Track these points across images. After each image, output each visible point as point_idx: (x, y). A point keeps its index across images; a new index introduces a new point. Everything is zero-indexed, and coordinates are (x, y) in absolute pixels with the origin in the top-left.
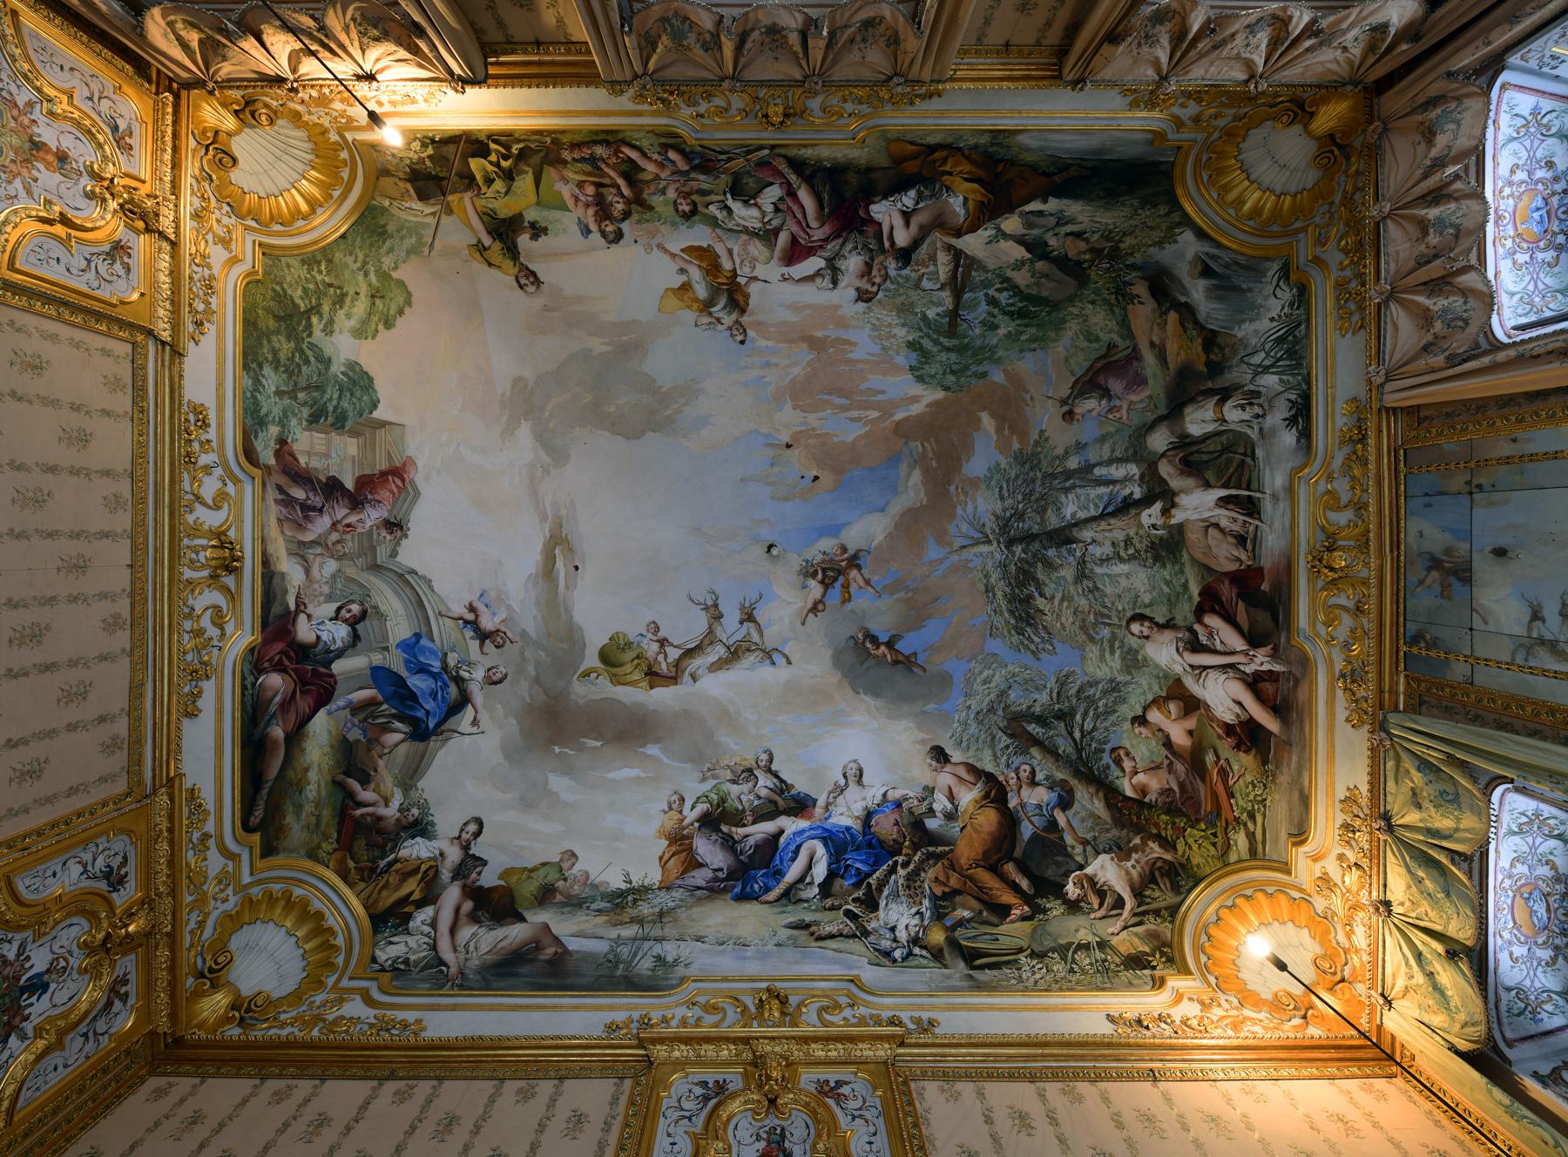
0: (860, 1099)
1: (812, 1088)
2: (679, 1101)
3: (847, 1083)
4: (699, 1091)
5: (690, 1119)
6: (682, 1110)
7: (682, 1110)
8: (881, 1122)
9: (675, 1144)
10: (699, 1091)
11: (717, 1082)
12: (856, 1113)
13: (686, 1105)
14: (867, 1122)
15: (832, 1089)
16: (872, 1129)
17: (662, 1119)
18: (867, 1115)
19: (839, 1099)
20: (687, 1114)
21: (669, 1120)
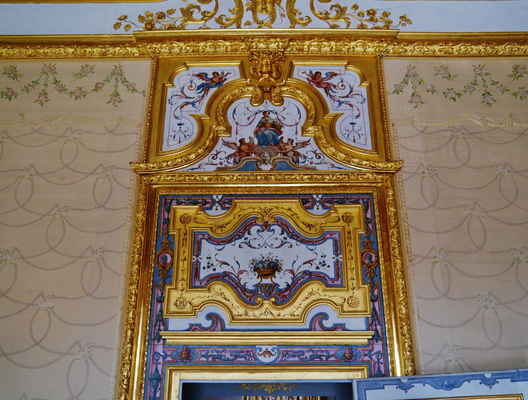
0: (348, 90)
3: (336, 75)
4: (199, 81)
5: (193, 104)
6: (187, 97)
7: (187, 97)
8: (365, 108)
10: (199, 81)
13: (187, 92)
14: (351, 105)
16: (356, 113)
17: (168, 106)
19: (328, 88)
21: (174, 107)
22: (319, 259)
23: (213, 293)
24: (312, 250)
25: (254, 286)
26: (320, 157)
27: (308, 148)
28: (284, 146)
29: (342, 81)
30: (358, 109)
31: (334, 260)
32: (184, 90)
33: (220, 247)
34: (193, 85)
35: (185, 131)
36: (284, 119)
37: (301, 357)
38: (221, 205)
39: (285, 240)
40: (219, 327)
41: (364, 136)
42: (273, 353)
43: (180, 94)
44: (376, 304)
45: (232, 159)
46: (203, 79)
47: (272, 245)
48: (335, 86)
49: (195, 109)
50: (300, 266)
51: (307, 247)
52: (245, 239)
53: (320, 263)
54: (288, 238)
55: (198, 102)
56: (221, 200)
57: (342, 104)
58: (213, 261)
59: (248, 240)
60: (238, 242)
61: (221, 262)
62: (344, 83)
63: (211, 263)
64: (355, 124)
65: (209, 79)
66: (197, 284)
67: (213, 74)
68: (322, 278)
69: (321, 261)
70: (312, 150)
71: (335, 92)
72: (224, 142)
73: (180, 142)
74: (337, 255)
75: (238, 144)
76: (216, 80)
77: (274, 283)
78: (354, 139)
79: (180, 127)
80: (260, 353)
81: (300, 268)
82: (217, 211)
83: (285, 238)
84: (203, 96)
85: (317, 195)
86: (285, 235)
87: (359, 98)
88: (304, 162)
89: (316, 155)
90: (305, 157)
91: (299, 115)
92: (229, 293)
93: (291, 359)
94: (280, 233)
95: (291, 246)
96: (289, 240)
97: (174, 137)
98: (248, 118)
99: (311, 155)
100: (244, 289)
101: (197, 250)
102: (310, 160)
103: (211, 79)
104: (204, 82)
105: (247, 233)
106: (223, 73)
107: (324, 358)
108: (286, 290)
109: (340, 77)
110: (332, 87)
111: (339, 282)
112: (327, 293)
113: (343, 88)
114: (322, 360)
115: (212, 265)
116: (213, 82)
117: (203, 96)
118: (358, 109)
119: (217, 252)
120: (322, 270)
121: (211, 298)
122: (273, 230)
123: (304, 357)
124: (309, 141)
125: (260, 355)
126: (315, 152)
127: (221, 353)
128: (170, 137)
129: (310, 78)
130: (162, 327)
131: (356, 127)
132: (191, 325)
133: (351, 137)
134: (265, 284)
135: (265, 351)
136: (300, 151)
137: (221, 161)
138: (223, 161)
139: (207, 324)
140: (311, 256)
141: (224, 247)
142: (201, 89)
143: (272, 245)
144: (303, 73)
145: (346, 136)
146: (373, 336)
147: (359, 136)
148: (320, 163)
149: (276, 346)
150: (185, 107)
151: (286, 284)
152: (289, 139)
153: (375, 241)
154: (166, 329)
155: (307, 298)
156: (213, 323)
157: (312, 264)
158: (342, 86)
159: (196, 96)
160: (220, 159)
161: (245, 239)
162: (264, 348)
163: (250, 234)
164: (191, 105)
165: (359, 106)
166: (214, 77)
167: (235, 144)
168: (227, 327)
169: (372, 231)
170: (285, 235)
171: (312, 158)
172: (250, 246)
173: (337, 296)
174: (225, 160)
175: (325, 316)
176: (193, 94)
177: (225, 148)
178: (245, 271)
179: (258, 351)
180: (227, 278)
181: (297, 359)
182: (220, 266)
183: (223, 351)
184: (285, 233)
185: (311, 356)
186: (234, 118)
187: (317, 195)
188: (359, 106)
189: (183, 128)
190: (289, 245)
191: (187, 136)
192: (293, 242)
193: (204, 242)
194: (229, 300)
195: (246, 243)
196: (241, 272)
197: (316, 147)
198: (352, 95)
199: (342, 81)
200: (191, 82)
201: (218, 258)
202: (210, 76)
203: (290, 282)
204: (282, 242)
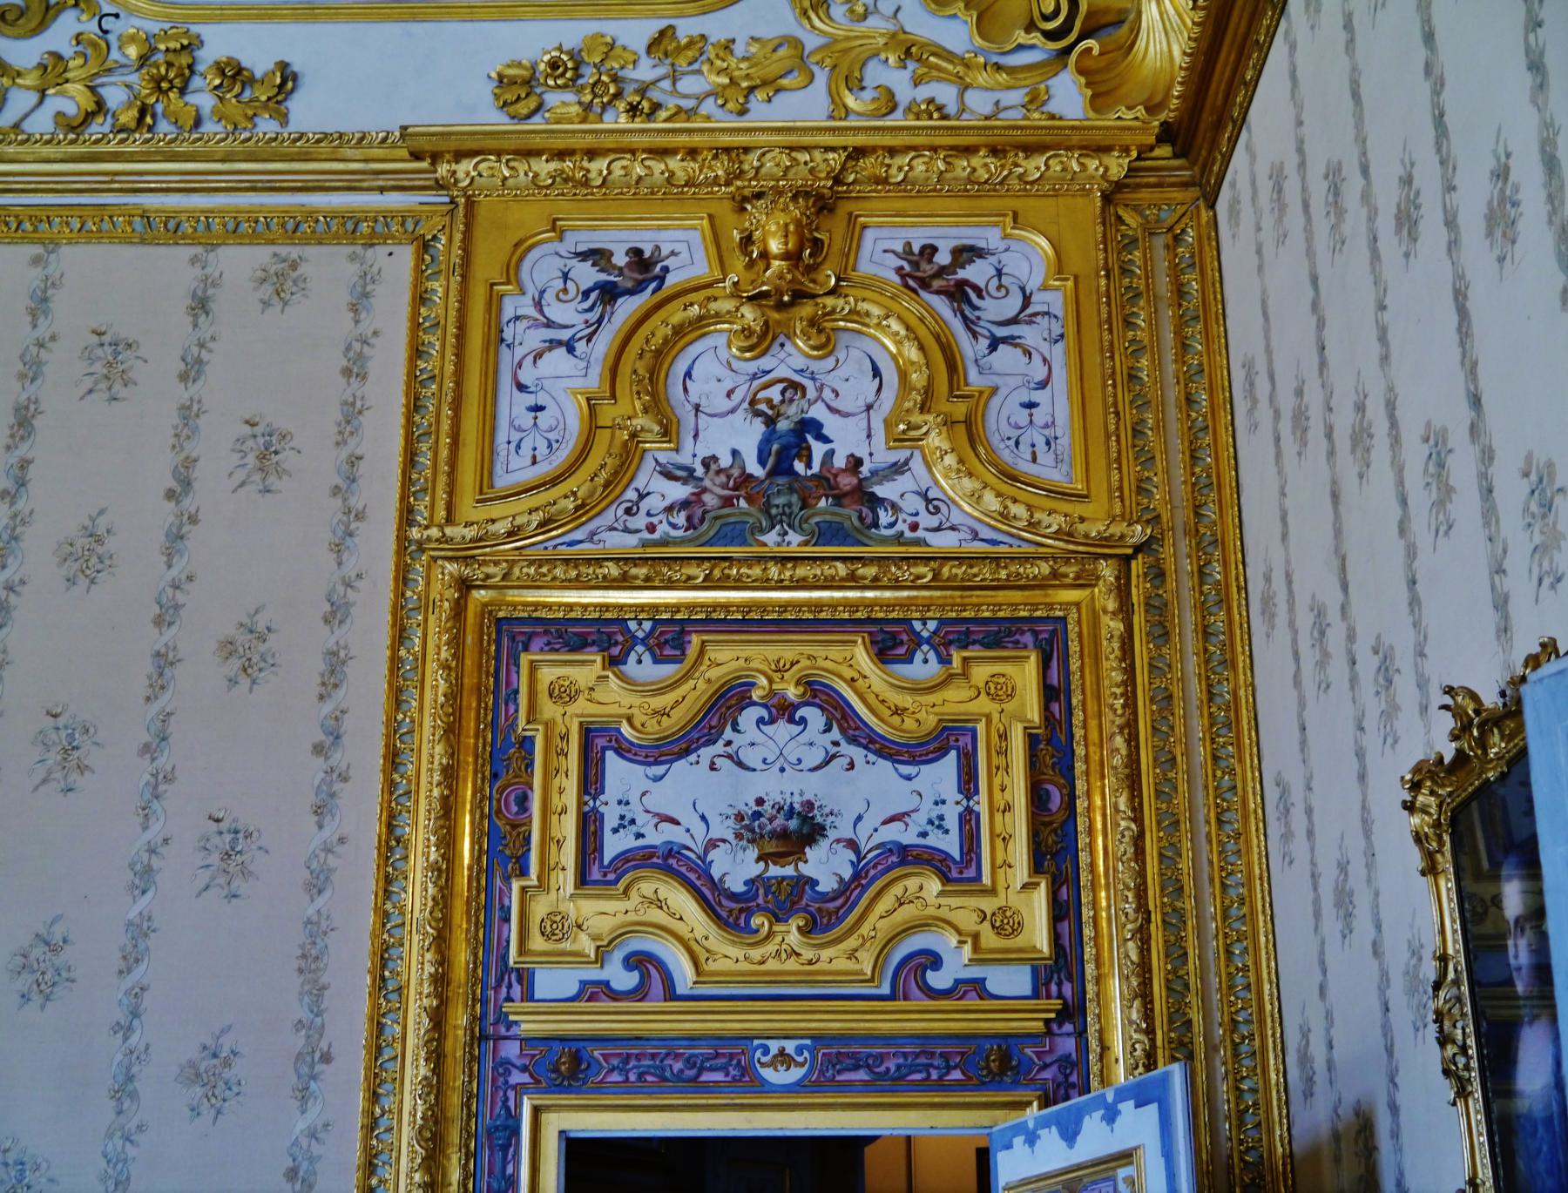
2: (538, 305)
4: (587, 274)
6: (550, 324)
7: (550, 324)
9: (539, 408)
10: (587, 274)
11: (636, 252)
12: (1001, 332)
13: (555, 312)
15: (942, 271)
16: (1040, 372)
20: (565, 335)
22: (927, 810)
24: (909, 778)
25: (746, 883)
29: (999, 273)
33: (659, 770)
37: (877, 1070)
40: (657, 986)
42: (800, 1059)
46: (602, 270)
47: (800, 761)
50: (876, 830)
51: (896, 769)
52: (725, 746)
53: (931, 822)
54: (843, 742)
55: (584, 341)
57: (1001, 347)
58: (635, 810)
59: (734, 746)
60: (706, 753)
62: (1005, 280)
63: (629, 817)
69: (934, 815)
73: (534, 462)
77: (804, 876)
78: (1034, 454)
79: (536, 418)
80: (764, 1059)
81: (874, 835)
83: (836, 744)
84: (600, 321)
85: (924, 621)
86: (835, 734)
91: (877, 380)
92: (681, 900)
94: (822, 728)
95: (852, 766)
101: (591, 781)
104: (603, 277)
105: (728, 728)
109: (992, 259)
110: (973, 296)
113: (1003, 291)
114: (929, 1074)
115: (633, 822)
117: (600, 321)
119: (649, 785)
120: (935, 840)
121: (632, 917)
123: (882, 1069)
125: (763, 1065)
127: (662, 1061)
129: (907, 268)
131: (1040, 415)
132: (584, 984)
134: (776, 878)
139: (626, 980)
141: (667, 771)
142: (593, 296)
143: (800, 761)
145: (1012, 443)
149: (808, 1042)
150: (547, 356)
155: (890, 913)
157: (907, 825)
158: (999, 287)
159: (578, 320)
161: (725, 746)
162: (774, 1050)
163: (739, 731)
164: (563, 350)
172: (740, 764)
175: (935, 961)
176: (568, 313)
178: (724, 841)
179: (758, 1054)
180: (672, 861)
181: (862, 1075)
182: (656, 826)
187: (924, 621)
190: (848, 760)
191: (555, 446)
192: (857, 753)
193: (610, 755)
194: (681, 919)
195: (729, 757)
196: (712, 844)
198: (1031, 315)
199: (999, 273)
202: (620, 259)
203: (847, 873)
204: (827, 752)
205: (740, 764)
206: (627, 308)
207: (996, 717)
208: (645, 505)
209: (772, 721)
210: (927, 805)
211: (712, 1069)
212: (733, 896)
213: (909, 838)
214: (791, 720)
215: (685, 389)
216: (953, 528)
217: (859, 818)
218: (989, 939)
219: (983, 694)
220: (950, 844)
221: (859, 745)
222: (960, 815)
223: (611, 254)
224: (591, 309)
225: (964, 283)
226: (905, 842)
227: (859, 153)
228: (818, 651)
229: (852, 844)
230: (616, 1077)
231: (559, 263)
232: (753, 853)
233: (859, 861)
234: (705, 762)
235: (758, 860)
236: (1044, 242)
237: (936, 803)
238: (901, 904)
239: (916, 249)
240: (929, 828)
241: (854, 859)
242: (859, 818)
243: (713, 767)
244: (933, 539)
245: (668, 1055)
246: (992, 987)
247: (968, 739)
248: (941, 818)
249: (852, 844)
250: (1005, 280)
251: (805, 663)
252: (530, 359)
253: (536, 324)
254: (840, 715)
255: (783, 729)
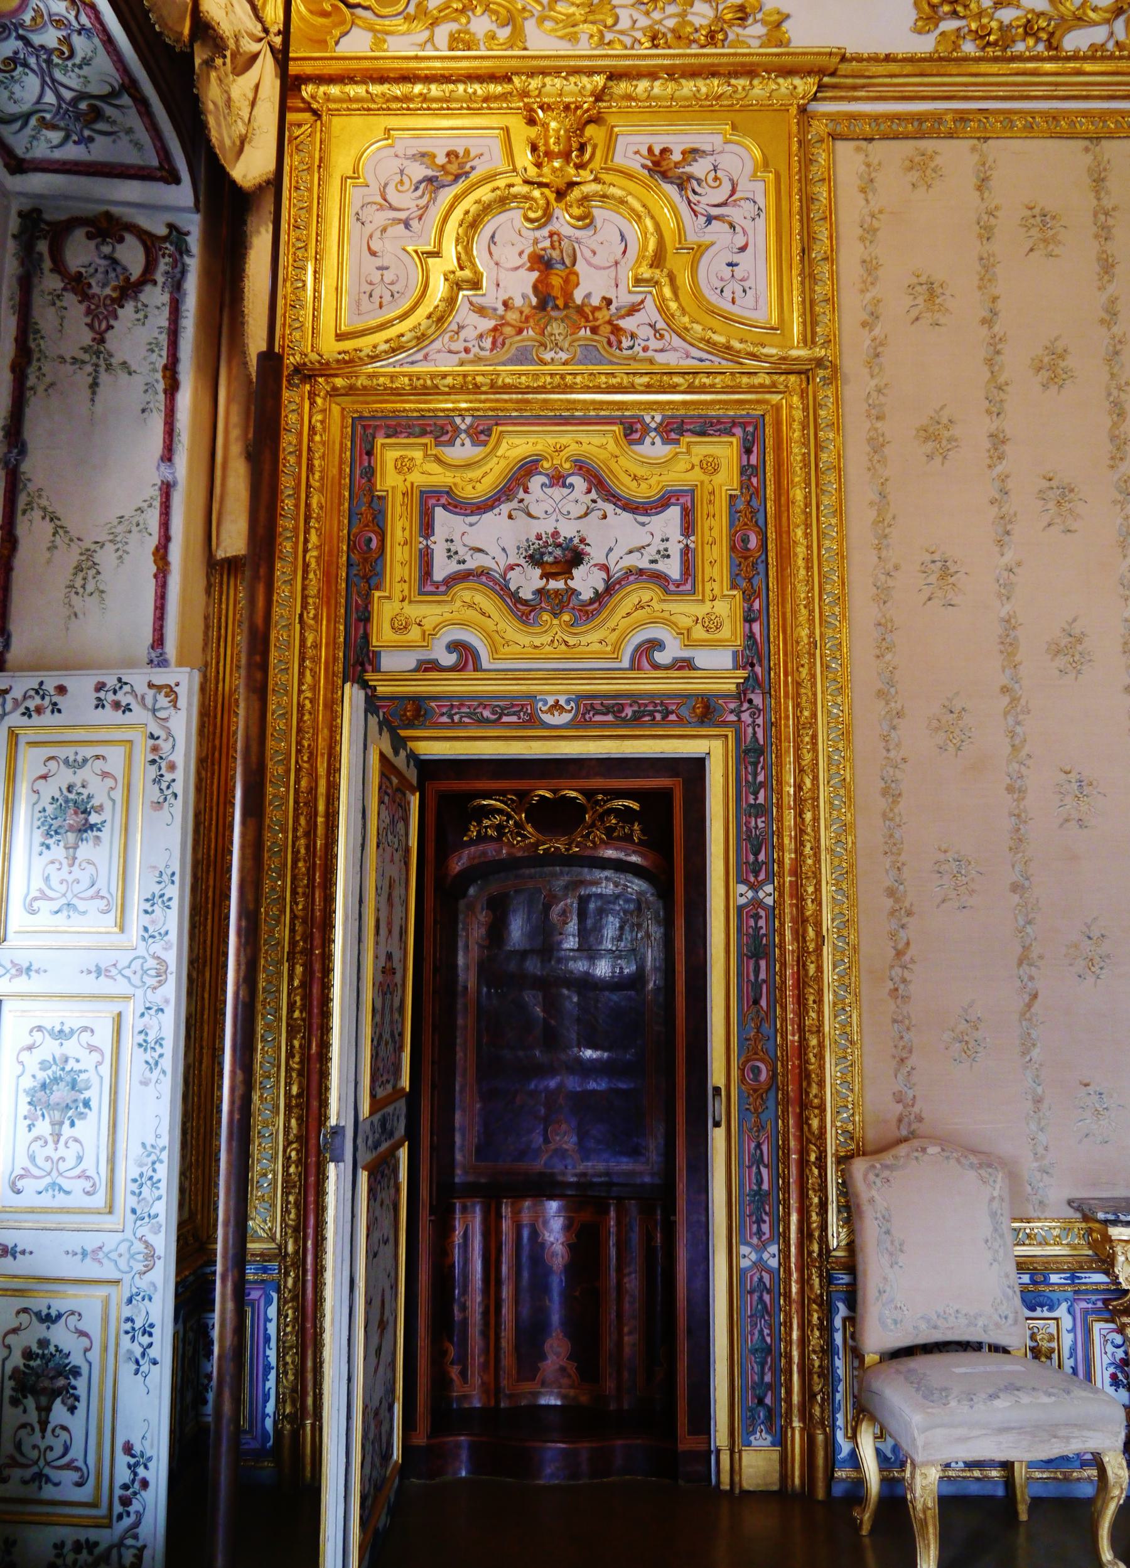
0: (727, 188)
1: (635, 164)
4: (419, 171)
5: (407, 225)
6: (392, 208)
7: (392, 208)
14: (732, 226)
16: (740, 241)
18: (733, 213)
20: (403, 215)
23: (458, 603)
24: (643, 524)
25: (534, 593)
26: (662, 336)
27: (639, 317)
28: (593, 313)
30: (745, 233)
31: (682, 546)
32: (387, 190)
34: (405, 179)
35: (392, 283)
36: (594, 253)
38: (470, 436)
39: (594, 505)
41: (753, 291)
42: (568, 708)
43: (379, 200)
44: (756, 627)
45: (490, 340)
46: (427, 168)
48: (699, 181)
49: (409, 234)
56: (470, 427)
57: (714, 222)
58: (457, 546)
59: (525, 503)
60: (505, 508)
61: (471, 549)
62: (719, 174)
63: (453, 549)
64: (737, 265)
65: (438, 166)
66: (429, 588)
67: (448, 155)
68: (659, 578)
70: (648, 321)
71: (700, 195)
72: (471, 303)
73: (381, 307)
74: (687, 536)
75: (501, 310)
76: (453, 168)
82: (462, 450)
83: (594, 501)
86: (593, 495)
87: (748, 205)
88: (631, 348)
89: (656, 331)
90: (633, 336)
93: (598, 718)
94: (585, 490)
95: (605, 517)
96: (601, 504)
97: (371, 296)
98: (521, 254)
99: (645, 332)
100: (515, 597)
101: (427, 527)
102: (643, 344)
103: (443, 167)
106: (467, 152)
107: (658, 716)
108: (592, 601)
109: (710, 159)
110: (694, 183)
111: (688, 587)
112: (665, 606)
114: (654, 718)
115: (456, 553)
116: (447, 173)
117: (427, 207)
118: (745, 233)
122: (571, 485)
124: (642, 302)
126: (652, 326)
128: (362, 295)
130: (370, 668)
133: (727, 294)
135: (552, 706)
136: (622, 323)
137: (466, 344)
138: (470, 345)
139: (449, 659)
140: (640, 537)
143: (569, 513)
144: (637, 153)
145: (718, 291)
146: (746, 679)
147: (744, 291)
148: (662, 351)
151: (592, 590)
152: (604, 298)
153: (762, 509)
154: (377, 669)
155: (628, 614)
156: (461, 655)
158: (716, 179)
159: (412, 205)
160: (465, 341)
162: (551, 702)
164: (402, 226)
165: (747, 225)
166: (450, 162)
167: (495, 309)
168: (485, 665)
169: (757, 489)
170: (593, 495)
171: (648, 340)
173: (684, 610)
174: (475, 343)
176: (407, 200)
177: (473, 318)
178: (518, 565)
179: (540, 704)
180: (484, 579)
181: (610, 718)
183: (479, 706)
184: (593, 490)
185: (634, 712)
186: (491, 253)
188: (747, 225)
189: (389, 276)
190: (601, 513)
191: (396, 295)
192: (609, 508)
193: (439, 511)
196: (511, 568)
197: (655, 316)
200: (402, 172)
201: (467, 540)
202: (441, 160)
203: (601, 587)
205: (529, 515)
206: (447, 195)
207: (706, 483)
208: (463, 334)
209: (551, 486)
210: (657, 539)
211: (507, 715)
212: (525, 603)
213: (644, 564)
214: (564, 485)
215: (491, 253)
216: (675, 350)
217: (611, 550)
218: (699, 633)
219: (697, 468)
220: (672, 568)
221: (610, 502)
222: (681, 550)
223: (434, 156)
224: (421, 197)
225: (690, 177)
226: (641, 567)
227: (614, 76)
228: (584, 439)
229: (605, 568)
230: (445, 719)
231: (397, 163)
232: (538, 572)
233: (609, 579)
234: (505, 514)
235: (541, 578)
236: (758, 154)
237: (663, 540)
238: (637, 609)
239: (657, 152)
240: (657, 557)
241: (605, 577)
242: (611, 550)
243: (510, 517)
244: (660, 358)
245: (479, 706)
246: (698, 663)
247: (689, 498)
248: (666, 550)
249: (605, 568)
250: (719, 174)
251: (574, 446)
252: (378, 234)
253: (381, 208)
254: (598, 482)
255: (557, 492)
